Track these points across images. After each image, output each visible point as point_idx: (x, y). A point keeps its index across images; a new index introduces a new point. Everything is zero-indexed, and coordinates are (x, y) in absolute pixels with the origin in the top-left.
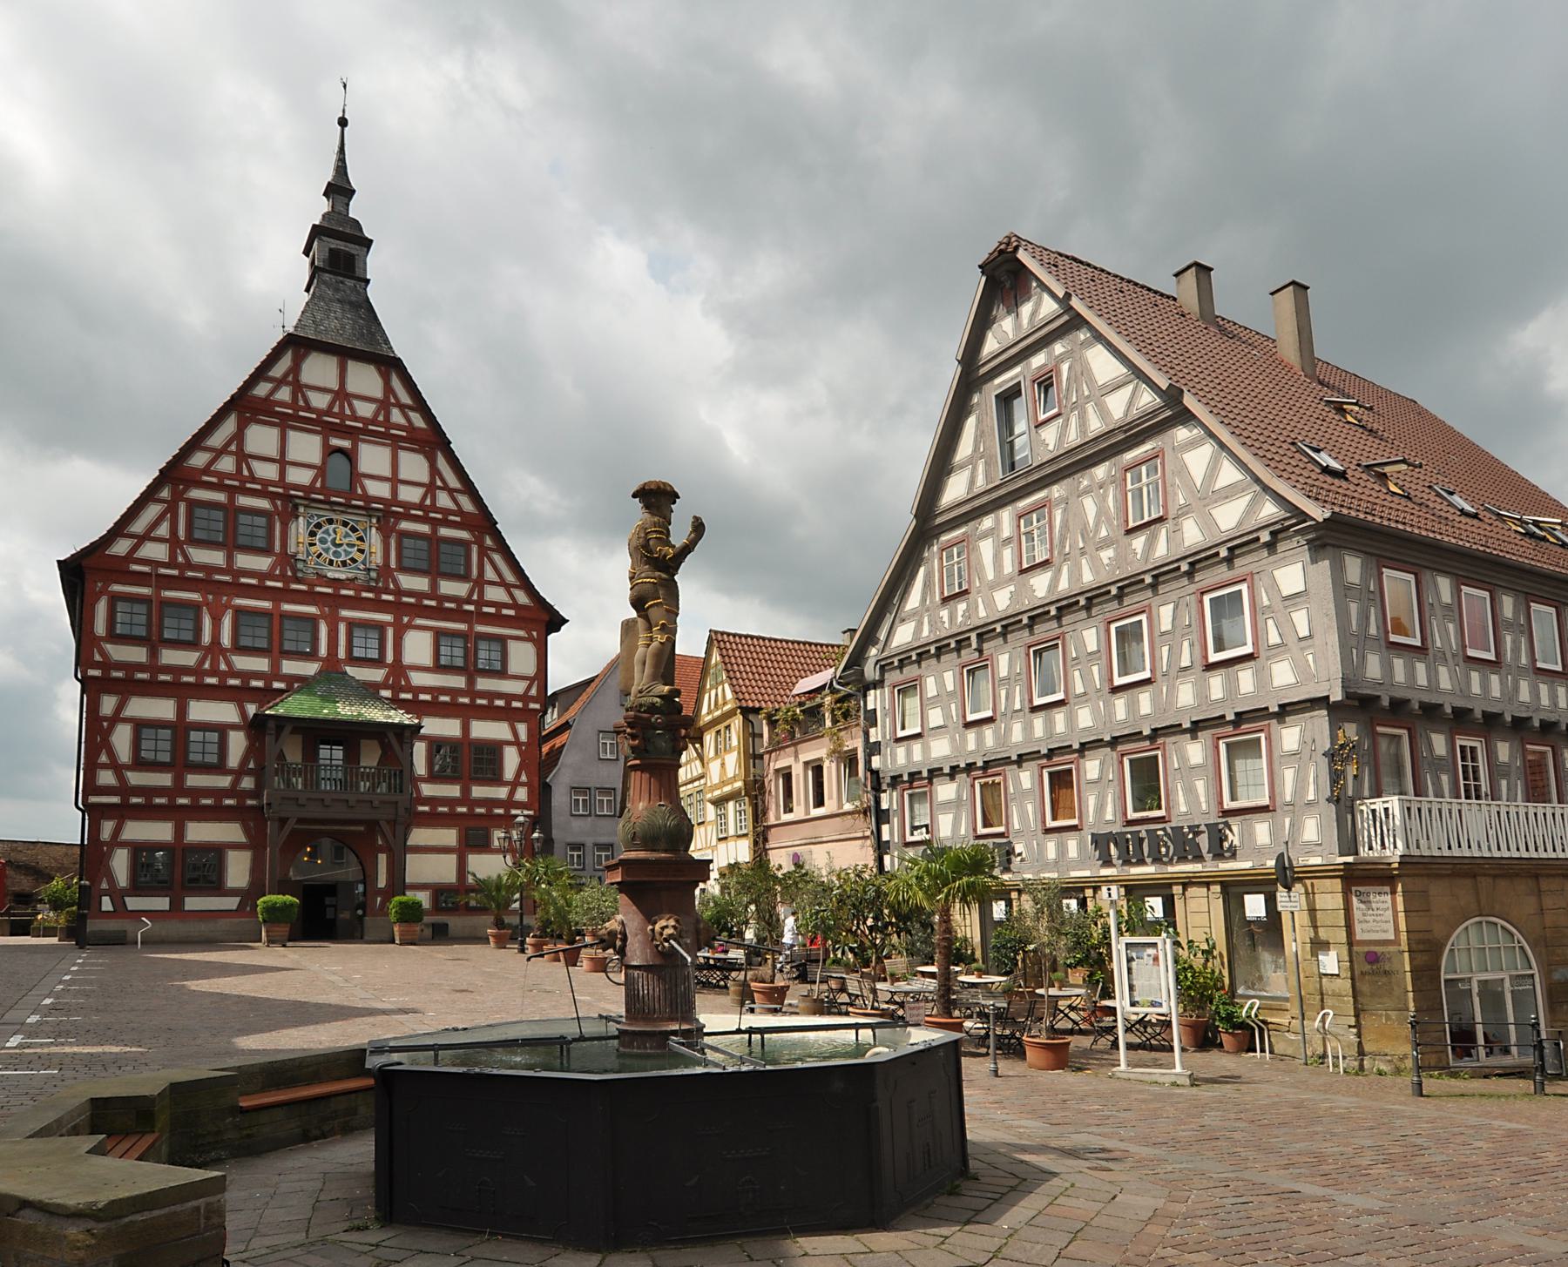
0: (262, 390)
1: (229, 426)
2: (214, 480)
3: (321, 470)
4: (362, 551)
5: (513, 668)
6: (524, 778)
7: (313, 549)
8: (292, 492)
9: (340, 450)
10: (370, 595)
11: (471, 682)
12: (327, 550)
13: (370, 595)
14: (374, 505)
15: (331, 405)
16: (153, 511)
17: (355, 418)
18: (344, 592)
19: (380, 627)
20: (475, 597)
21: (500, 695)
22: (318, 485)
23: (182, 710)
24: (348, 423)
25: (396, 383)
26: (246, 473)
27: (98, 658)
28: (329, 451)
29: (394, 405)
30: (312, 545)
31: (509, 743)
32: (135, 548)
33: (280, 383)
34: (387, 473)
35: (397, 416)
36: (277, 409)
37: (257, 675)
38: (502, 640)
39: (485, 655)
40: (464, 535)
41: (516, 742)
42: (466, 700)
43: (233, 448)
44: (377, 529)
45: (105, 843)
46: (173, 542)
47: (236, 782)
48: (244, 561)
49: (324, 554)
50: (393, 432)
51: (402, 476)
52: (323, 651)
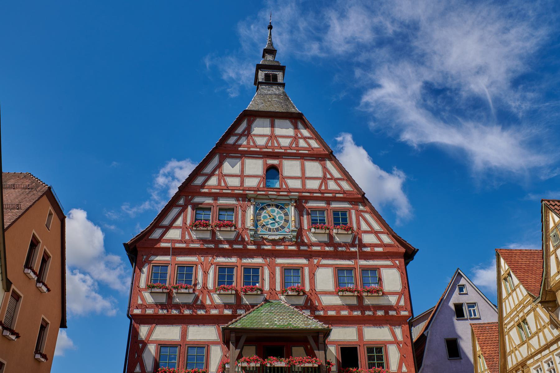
0: (231, 140)
1: (215, 161)
8: (247, 192)
21: (380, 307)
24: (276, 150)
26: (223, 184)
27: (140, 302)
31: (391, 343)
34: (299, 174)
35: (302, 143)
36: (240, 149)
40: (346, 205)
51: (308, 174)
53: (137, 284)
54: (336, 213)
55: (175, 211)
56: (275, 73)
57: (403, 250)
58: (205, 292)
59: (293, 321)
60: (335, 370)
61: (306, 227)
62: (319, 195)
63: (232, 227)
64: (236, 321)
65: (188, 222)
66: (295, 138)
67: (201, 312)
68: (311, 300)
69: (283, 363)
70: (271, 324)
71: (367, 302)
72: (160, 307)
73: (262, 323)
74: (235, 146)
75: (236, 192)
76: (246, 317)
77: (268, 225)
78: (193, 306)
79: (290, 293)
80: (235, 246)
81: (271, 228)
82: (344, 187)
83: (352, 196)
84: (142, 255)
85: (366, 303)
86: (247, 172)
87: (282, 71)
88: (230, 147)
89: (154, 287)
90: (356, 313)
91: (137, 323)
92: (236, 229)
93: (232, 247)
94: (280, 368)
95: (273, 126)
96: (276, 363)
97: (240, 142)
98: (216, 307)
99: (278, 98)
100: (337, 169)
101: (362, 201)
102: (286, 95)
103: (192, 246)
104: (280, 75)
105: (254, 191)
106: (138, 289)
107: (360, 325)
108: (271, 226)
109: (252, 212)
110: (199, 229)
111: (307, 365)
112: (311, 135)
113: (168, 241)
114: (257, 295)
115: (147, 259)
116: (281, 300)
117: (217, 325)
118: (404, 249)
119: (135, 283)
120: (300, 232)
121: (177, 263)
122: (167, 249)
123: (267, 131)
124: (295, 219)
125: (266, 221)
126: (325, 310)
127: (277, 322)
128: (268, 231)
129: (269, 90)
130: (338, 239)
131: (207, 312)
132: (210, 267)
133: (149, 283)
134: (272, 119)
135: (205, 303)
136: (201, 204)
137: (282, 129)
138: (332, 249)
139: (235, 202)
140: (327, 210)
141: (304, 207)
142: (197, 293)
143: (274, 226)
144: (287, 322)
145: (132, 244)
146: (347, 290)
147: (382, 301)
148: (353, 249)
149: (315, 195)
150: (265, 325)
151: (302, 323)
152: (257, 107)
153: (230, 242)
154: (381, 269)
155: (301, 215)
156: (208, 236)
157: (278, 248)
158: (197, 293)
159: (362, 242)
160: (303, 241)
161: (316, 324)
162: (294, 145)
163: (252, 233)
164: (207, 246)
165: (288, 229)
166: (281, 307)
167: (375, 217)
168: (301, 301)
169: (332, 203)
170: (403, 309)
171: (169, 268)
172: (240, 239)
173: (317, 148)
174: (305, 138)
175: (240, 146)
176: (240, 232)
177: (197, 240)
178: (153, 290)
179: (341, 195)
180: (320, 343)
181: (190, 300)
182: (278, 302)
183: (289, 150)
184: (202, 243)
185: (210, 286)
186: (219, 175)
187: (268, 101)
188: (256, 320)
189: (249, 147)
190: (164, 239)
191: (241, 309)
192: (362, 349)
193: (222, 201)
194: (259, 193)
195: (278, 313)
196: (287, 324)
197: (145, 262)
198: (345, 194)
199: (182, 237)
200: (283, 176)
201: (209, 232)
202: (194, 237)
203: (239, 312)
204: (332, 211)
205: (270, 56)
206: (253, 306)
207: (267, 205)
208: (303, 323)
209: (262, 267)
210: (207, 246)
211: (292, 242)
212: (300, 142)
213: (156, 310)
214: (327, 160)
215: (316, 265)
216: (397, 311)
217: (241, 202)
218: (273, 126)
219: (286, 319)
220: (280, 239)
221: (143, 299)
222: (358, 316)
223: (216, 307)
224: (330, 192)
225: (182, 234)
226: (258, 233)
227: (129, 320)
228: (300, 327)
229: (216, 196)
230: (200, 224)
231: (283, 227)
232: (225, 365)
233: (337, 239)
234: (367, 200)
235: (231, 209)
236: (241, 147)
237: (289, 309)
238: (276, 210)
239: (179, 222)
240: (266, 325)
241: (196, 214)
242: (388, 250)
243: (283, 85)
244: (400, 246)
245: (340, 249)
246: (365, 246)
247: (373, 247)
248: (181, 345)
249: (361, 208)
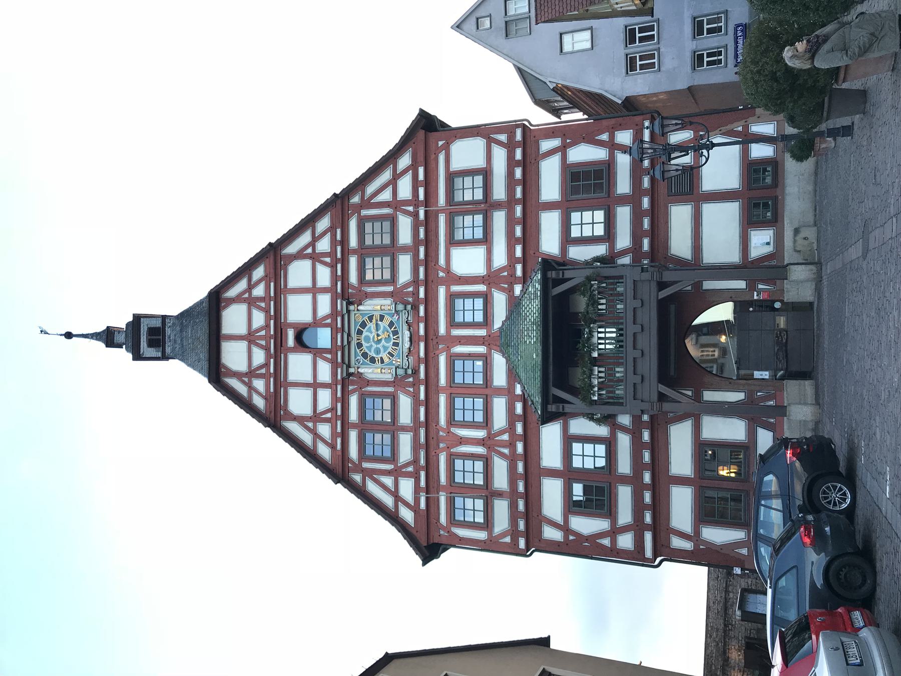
0: (259, 402)
1: (293, 427)
2: (339, 440)
3: (317, 353)
4: (382, 318)
5: (479, 162)
6: (605, 137)
7: (386, 360)
8: (339, 377)
9: (299, 338)
10: (422, 309)
11: (498, 205)
12: (385, 348)
13: (422, 309)
15: (261, 347)
16: (373, 488)
17: (267, 326)
18: (422, 332)
19: (451, 298)
20: (411, 209)
21: (510, 174)
22: (329, 356)
23: (552, 473)
25: (232, 292)
27: (508, 539)
28: (301, 344)
29: (250, 294)
30: (382, 361)
31: (564, 158)
32: (406, 504)
33: (251, 388)
34: (308, 297)
35: (259, 291)
36: (272, 390)
37: (511, 409)
38: (451, 177)
39: (471, 191)
40: (353, 224)
41: (563, 150)
42: (519, 210)
43: (310, 425)
44: (360, 304)
46: (397, 473)
47: (624, 429)
48: (405, 417)
49: (390, 350)
50: (272, 294)
51: (308, 283)
52: (481, 349)
59: (530, 316)
67: (520, 448)
74: (269, 398)
76: (526, 387)
82: (326, 227)
84: (440, 536)
99: (187, 326)
113: (417, 500)
122: (428, 500)
127: (532, 340)
128: (398, 346)
129: (175, 340)
134: (221, 339)
151: (532, 303)
162: (263, 305)
165: (393, 316)
170: (512, 135)
174: (251, 287)
183: (270, 313)
197: (448, 532)
199: (411, 477)
203: (518, 390)
208: (532, 301)
219: (528, 326)
220: (409, 329)
224: (334, 249)
247: (418, 182)
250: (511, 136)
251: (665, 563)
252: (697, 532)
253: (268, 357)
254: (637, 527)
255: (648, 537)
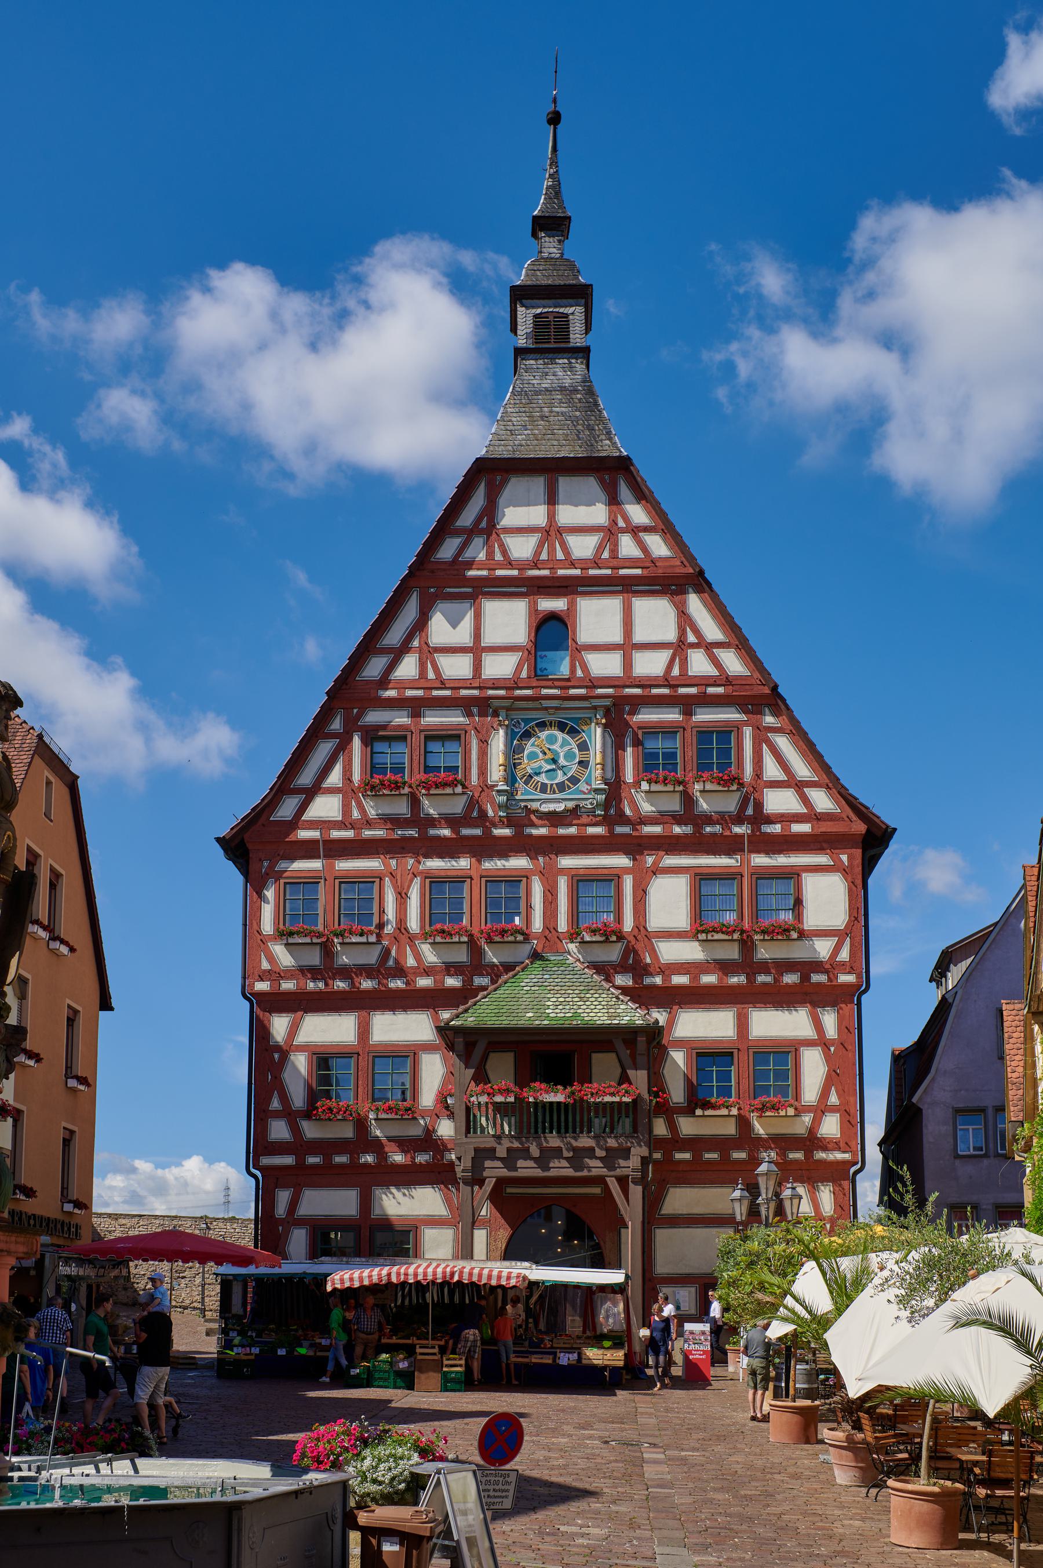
0: (447, 550)
5: (812, 920)
6: (834, 1099)
8: (491, 692)
14: (600, 691)
15: (538, 553)
19: (613, 878)
21: (790, 966)
24: (561, 572)
26: (431, 675)
27: (265, 965)
29: (624, 531)
31: (809, 1043)
33: (470, 533)
34: (617, 638)
35: (627, 547)
36: (471, 573)
38: (793, 875)
40: (732, 715)
41: (821, 1042)
45: (281, 1221)
51: (640, 635)
53: (255, 926)
54: (705, 734)
55: (324, 749)
56: (562, 310)
57: (860, 827)
58: (403, 939)
60: (682, 1100)
61: (629, 777)
62: (665, 691)
63: (456, 786)
64: (466, 1011)
65: (356, 777)
66: (610, 533)
67: (397, 984)
68: (636, 953)
69: (559, 1095)
70: (537, 1015)
71: (762, 954)
72: (309, 975)
73: (519, 1015)
74: (456, 567)
75: (464, 692)
76: (487, 1000)
77: (538, 774)
78: (379, 971)
79: (587, 938)
80: (466, 832)
81: (546, 785)
83: (746, 690)
85: (759, 956)
86: (487, 640)
87: (583, 301)
88: (445, 570)
89: (293, 934)
90: (734, 980)
91: (264, 1011)
92: (467, 788)
93: (457, 832)
94: (555, 1105)
95: (552, 500)
96: (546, 1096)
97: (468, 554)
98: (427, 972)
99: (570, 402)
100: (714, 617)
101: (774, 702)
102: (590, 392)
103: (368, 833)
104: (575, 313)
105: (507, 688)
106: (259, 937)
107: (743, 1006)
108: (548, 779)
109: (502, 746)
110: (381, 793)
111: (608, 1099)
112: (652, 518)
113: (313, 825)
114: (515, 942)
115: (272, 866)
116: (570, 954)
117: (434, 1009)
118: (863, 824)
119: (251, 924)
120: (614, 789)
121: (337, 874)
122: (314, 842)
123: (536, 515)
124: (604, 757)
125: (535, 765)
126: (667, 973)
130: (705, 806)
131: (410, 984)
132: (411, 881)
133: (281, 926)
135: (403, 963)
136: (384, 727)
137: (576, 506)
138: (688, 829)
139: (462, 719)
140: (684, 729)
141: (627, 725)
142: (385, 943)
143: (553, 779)
144: (572, 1011)
145: (234, 837)
146: (714, 930)
147: (797, 952)
148: (737, 830)
149: (655, 691)
150: (525, 1018)
152: (511, 443)
153: (453, 822)
154: (804, 875)
155: (619, 746)
156: (401, 808)
157: (562, 831)
158: (385, 943)
159: (762, 810)
160: (621, 813)
161: (633, 1014)
163: (502, 799)
164: (403, 833)
165: (587, 783)
166: (566, 972)
167: (801, 743)
168: (613, 953)
169: (698, 710)
171: (322, 892)
172: (475, 814)
173: (666, 559)
174: (635, 531)
175: (470, 564)
176: (477, 795)
177: (379, 821)
178: (291, 941)
179: (720, 690)
180: (644, 1054)
181: (371, 957)
182: (562, 958)
183: (592, 568)
184: (391, 827)
185: (413, 924)
186: (420, 650)
187: (542, 417)
188: (507, 1007)
189: (492, 567)
190: (304, 821)
191: (481, 975)
192: (743, 1056)
193: (432, 719)
194: (518, 692)
195: (556, 988)
196: (571, 1015)
197: (267, 874)
198: (731, 687)
200: (577, 644)
201: (405, 798)
202: (372, 813)
203: (479, 981)
204: (694, 733)
205: (551, 240)
206: (509, 967)
207: (537, 725)
209: (527, 878)
210: (403, 833)
211: (595, 816)
212: (623, 543)
213: (302, 982)
214: (690, 590)
215: (652, 868)
216: (831, 975)
217: (477, 718)
218: (552, 500)
219: (571, 1003)
221: (271, 959)
222: (738, 987)
223: (427, 972)
225: (343, 805)
226: (517, 798)
227: (247, 1004)
228: (598, 1022)
229: (416, 707)
230: (382, 784)
231: (574, 780)
232: (446, 1098)
233: (704, 805)
234: (784, 700)
235: (452, 736)
236: (474, 567)
237: (583, 976)
238: (560, 735)
239: (335, 777)
240: (528, 1018)
241: (372, 753)
242: (823, 830)
243: (584, 352)
244: (854, 817)
245: (708, 829)
246: (770, 820)
247: (788, 823)
248: (358, 1054)
249: (769, 720)
250: (844, 967)
251: (253, 1181)
252: (301, 1222)
253: (523, 566)
254: (299, 1146)
255: (289, 1160)
